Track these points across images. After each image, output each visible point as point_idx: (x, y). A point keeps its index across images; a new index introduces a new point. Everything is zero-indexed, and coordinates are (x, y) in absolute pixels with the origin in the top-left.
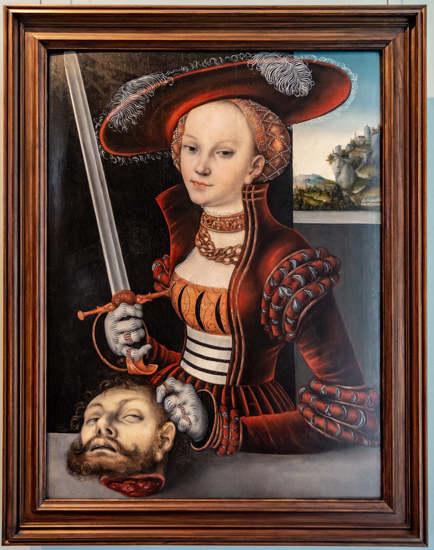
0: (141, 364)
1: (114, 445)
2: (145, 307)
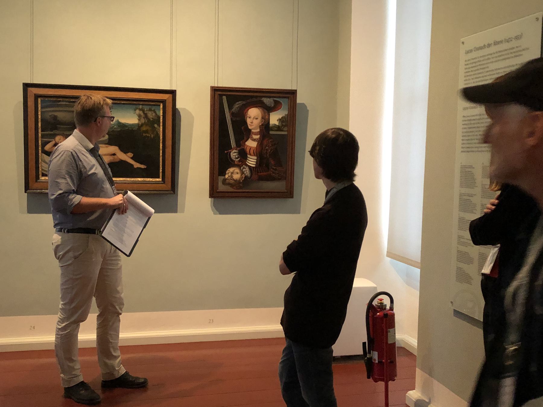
0: (238, 162)
1: (232, 179)
2: (239, 151)
